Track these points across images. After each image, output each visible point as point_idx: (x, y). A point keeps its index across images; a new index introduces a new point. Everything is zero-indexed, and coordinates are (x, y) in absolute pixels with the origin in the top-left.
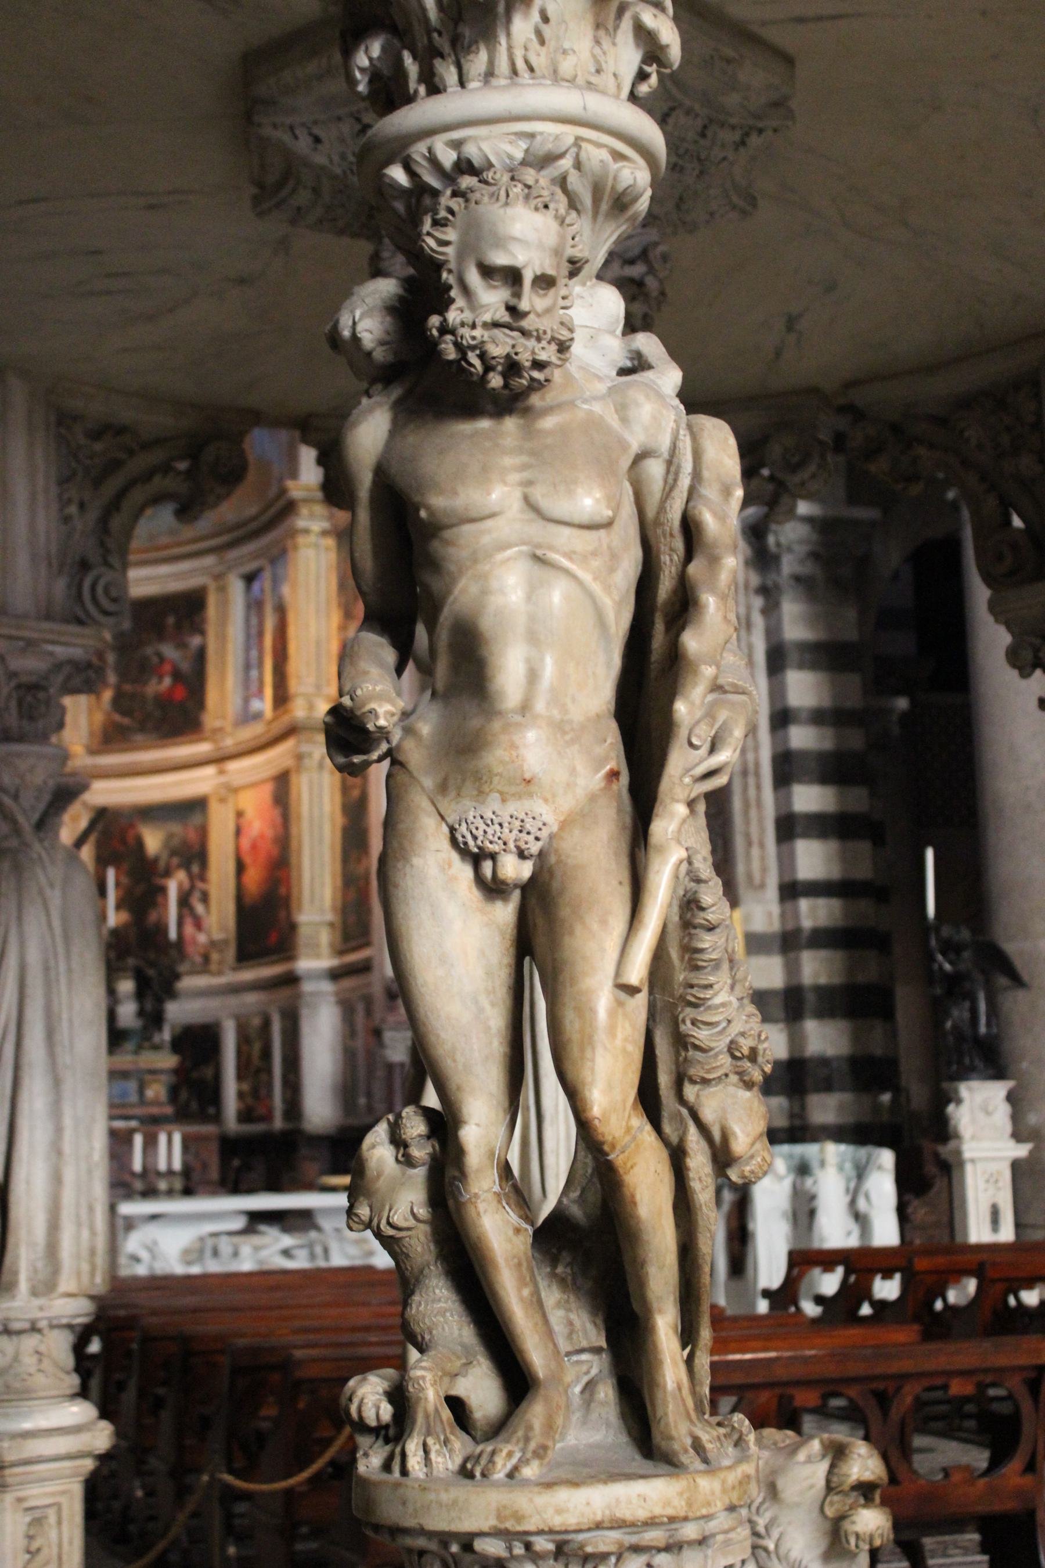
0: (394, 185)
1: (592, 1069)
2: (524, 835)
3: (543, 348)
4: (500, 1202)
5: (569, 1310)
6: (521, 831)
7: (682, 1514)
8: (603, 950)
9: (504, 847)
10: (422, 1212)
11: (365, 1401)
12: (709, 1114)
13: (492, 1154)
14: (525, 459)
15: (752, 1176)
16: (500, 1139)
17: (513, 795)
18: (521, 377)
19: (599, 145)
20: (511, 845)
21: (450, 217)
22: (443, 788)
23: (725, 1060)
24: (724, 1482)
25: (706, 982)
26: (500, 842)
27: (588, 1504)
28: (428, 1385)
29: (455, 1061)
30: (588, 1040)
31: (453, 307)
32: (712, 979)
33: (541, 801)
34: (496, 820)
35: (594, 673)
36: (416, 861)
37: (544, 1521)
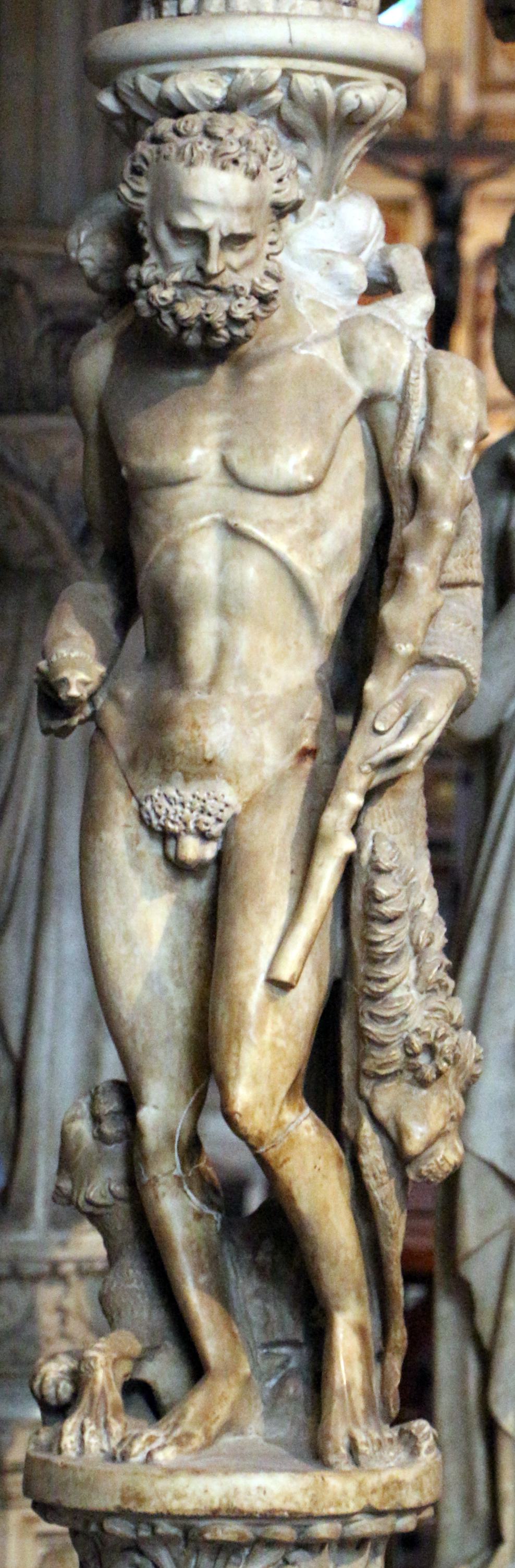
1: (237, 1064)
3: (240, 306)
4: (180, 1185)
5: (266, 1301)
7: (306, 1510)
8: (259, 943)
11: (47, 1379)
12: (382, 1109)
13: (172, 1137)
14: (227, 416)
15: (430, 1175)
16: (181, 1121)
17: (195, 775)
18: (218, 336)
20: (192, 826)
21: (144, 166)
22: (133, 761)
24: (360, 1484)
25: (380, 976)
26: (180, 822)
27: (206, 1491)
28: (98, 1366)
29: (134, 1041)
30: (236, 1034)
31: (147, 262)
32: (386, 972)
33: (224, 781)
35: (296, 643)
36: (105, 835)
37: (164, 1505)
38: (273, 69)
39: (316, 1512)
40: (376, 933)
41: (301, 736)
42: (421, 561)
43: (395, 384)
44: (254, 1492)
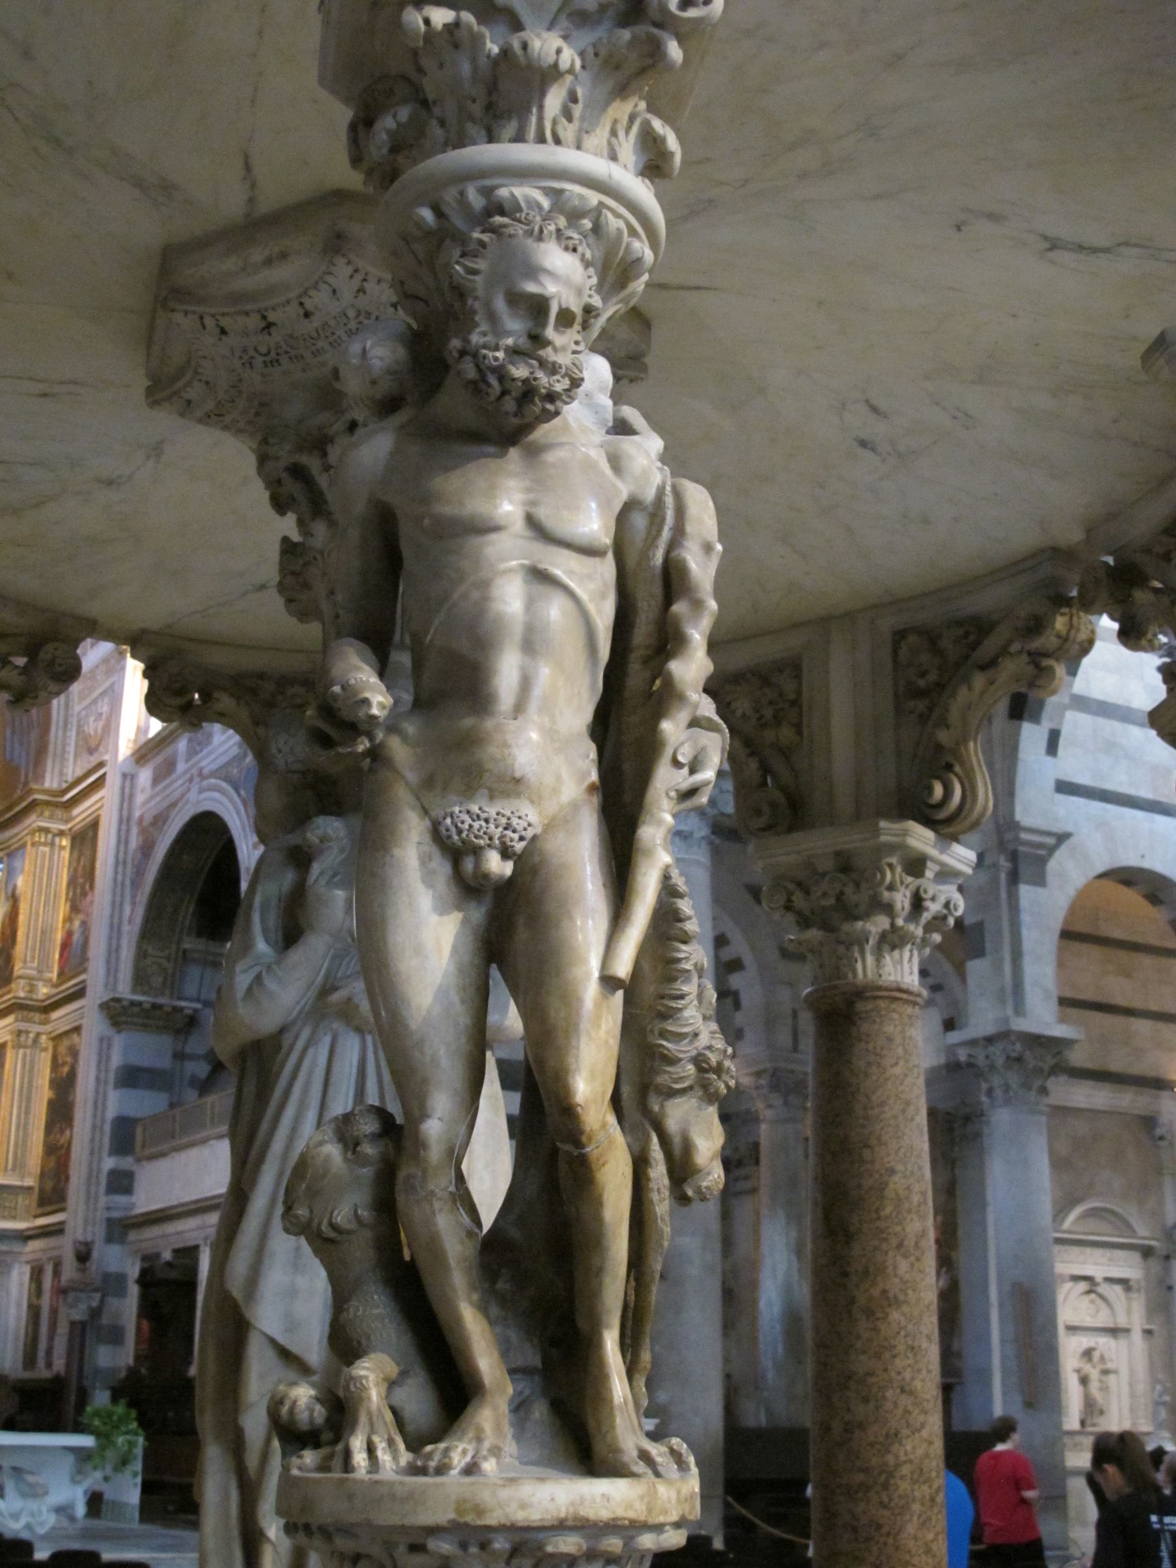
0: (420, 223)
1: (577, 1057)
2: (509, 833)
4: (454, 1202)
6: (506, 829)
9: (489, 842)
10: (364, 1213)
12: (672, 1124)
16: (460, 1138)
19: (618, 216)
22: (429, 782)
23: (691, 1068)
24: (679, 1492)
25: (679, 993)
27: (553, 1499)
28: (371, 1385)
30: (571, 1028)
31: (477, 330)
33: (527, 802)
34: (483, 815)
36: (397, 852)
38: (594, 198)
39: (651, 1521)
40: (679, 951)
41: (589, 774)
42: (695, 628)
43: (650, 495)
44: (598, 1500)
